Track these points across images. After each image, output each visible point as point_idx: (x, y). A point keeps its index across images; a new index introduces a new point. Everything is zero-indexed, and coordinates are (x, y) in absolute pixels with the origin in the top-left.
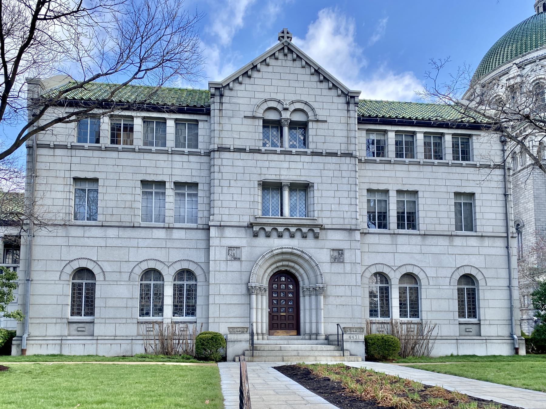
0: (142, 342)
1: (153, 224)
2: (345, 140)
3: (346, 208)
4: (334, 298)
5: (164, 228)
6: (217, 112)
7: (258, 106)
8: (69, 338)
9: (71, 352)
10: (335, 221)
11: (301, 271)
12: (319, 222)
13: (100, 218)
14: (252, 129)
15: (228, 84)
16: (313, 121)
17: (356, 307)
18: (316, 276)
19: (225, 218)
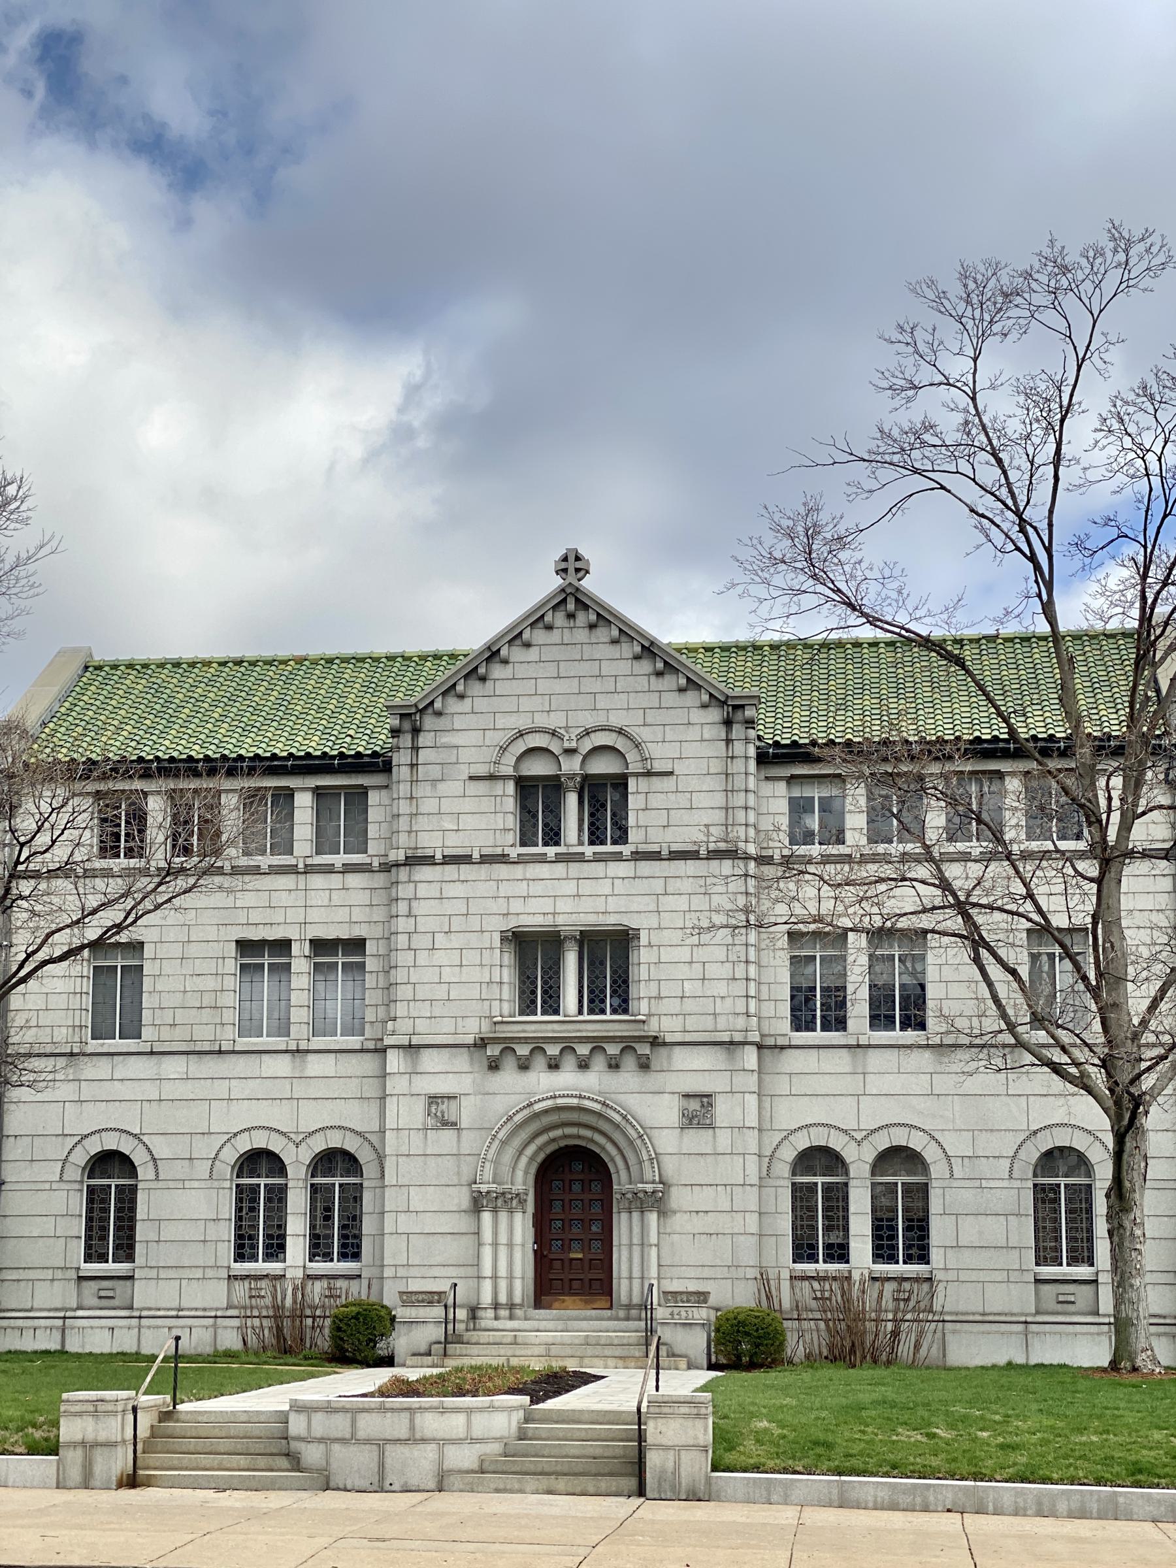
0: (236, 1323)
1: (265, 1041)
2: (719, 817)
3: (721, 988)
5: (286, 1051)
6: (405, 772)
7: (503, 749)
8: (80, 1313)
9: (83, 1347)
10: (691, 1023)
12: (653, 1028)
13: (146, 1033)
14: (487, 804)
15: (432, 702)
16: (637, 775)
17: (742, 1238)
18: (640, 1162)
19: (421, 1025)
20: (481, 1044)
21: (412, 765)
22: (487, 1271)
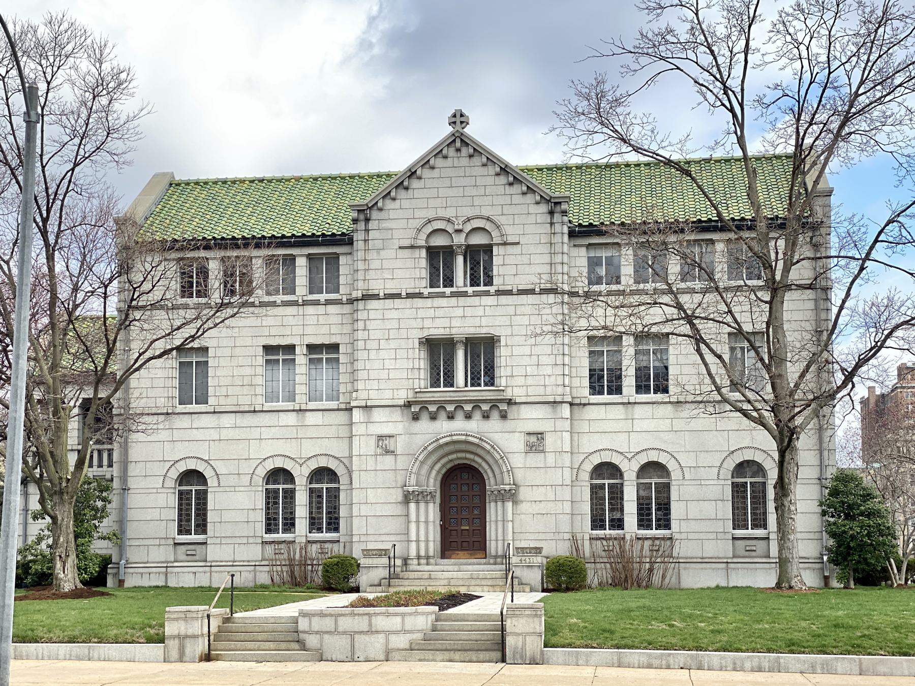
1: (281, 405)
2: (547, 268)
3: (548, 370)
4: (529, 504)
5: (294, 411)
6: (361, 243)
7: (419, 230)
10: (531, 391)
11: (484, 464)
12: (508, 394)
13: (211, 400)
14: (410, 263)
16: (498, 244)
17: (561, 516)
19: (373, 394)
20: (408, 405)
21: (365, 240)
22: (413, 537)
